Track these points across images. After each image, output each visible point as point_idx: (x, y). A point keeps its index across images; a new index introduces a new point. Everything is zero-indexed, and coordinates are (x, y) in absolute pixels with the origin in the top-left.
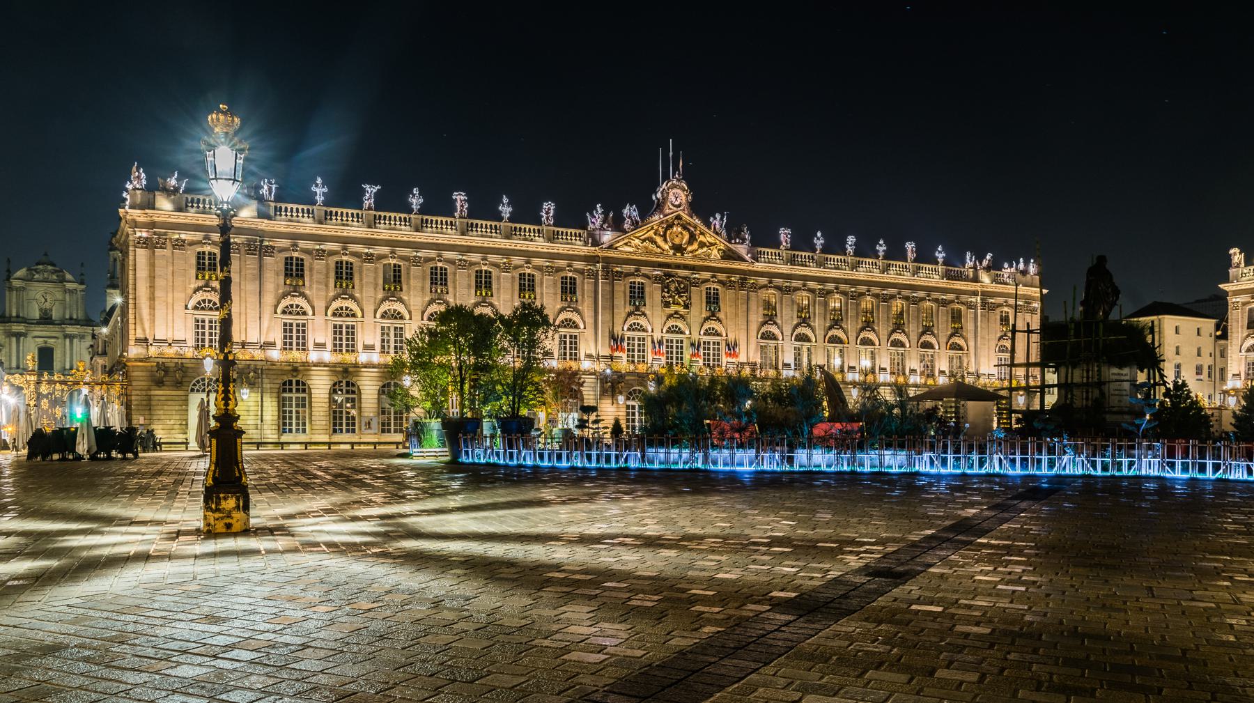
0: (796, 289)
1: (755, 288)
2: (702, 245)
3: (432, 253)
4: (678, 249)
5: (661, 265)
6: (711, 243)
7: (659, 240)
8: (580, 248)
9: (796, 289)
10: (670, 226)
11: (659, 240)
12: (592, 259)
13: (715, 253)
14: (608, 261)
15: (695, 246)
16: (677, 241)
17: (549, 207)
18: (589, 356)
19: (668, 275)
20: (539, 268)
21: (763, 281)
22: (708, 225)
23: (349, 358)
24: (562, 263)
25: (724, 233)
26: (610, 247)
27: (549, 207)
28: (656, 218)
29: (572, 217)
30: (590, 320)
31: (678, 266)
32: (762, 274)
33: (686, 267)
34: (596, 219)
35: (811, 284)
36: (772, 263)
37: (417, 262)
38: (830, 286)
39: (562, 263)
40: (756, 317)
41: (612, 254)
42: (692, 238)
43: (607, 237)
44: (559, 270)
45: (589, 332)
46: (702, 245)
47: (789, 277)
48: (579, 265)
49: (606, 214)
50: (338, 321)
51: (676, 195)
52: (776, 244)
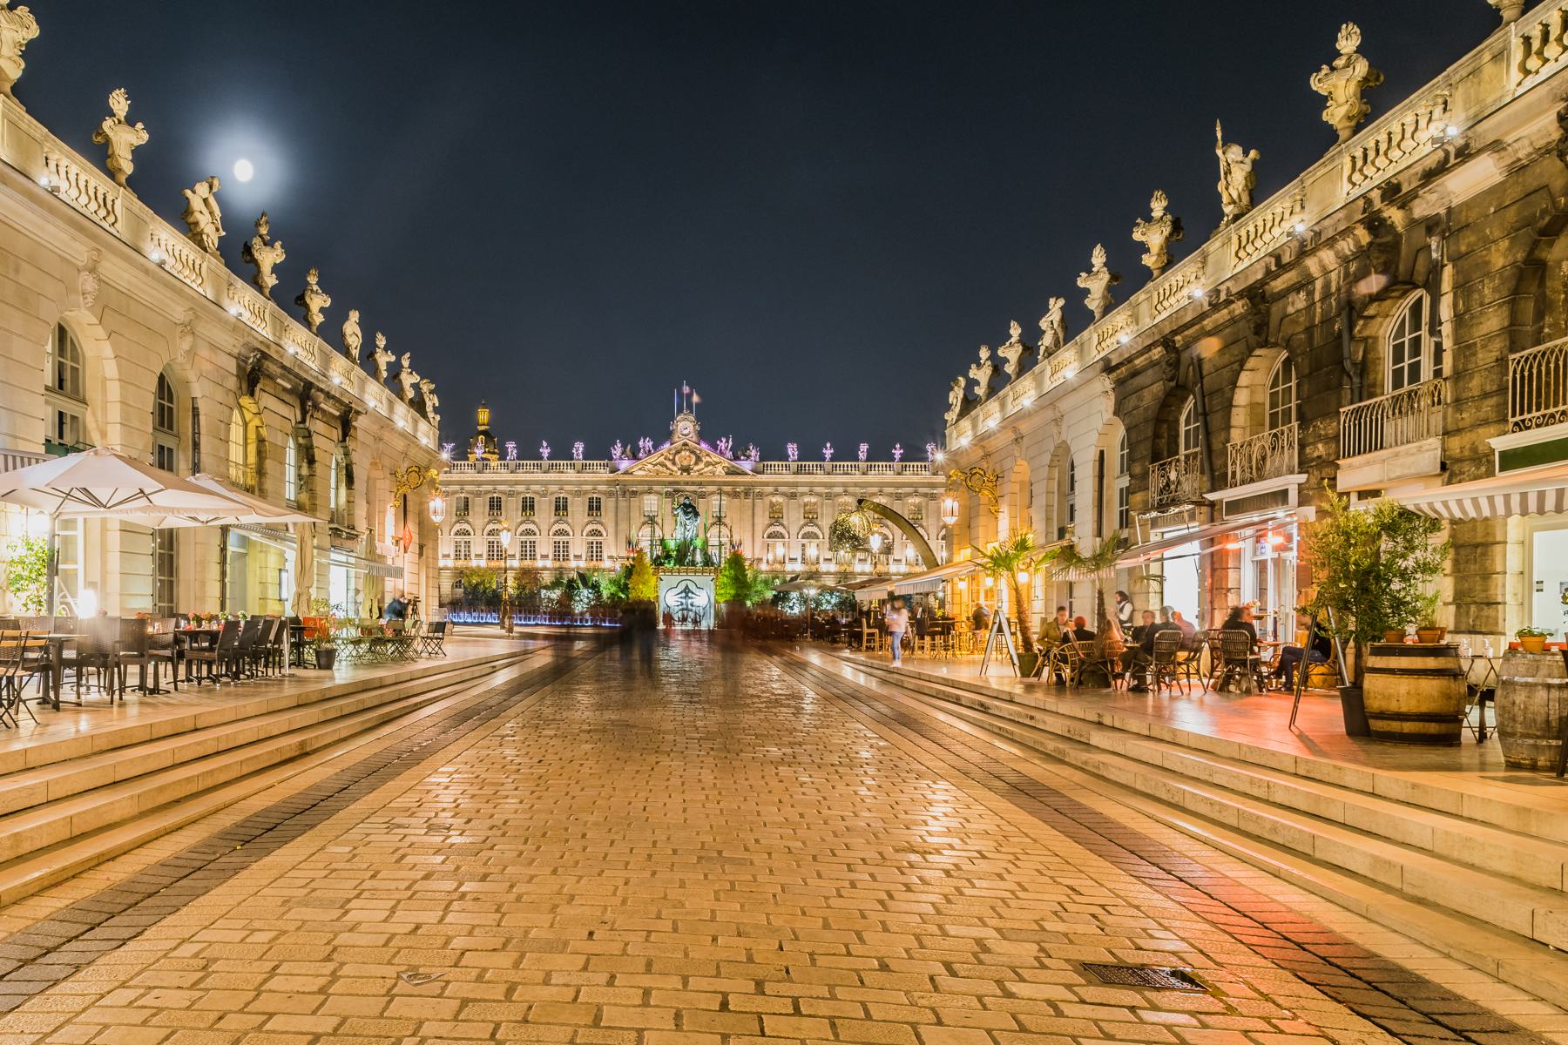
0: (803, 494)
1: (761, 495)
2: (708, 464)
3: (490, 488)
4: (686, 470)
5: (671, 483)
6: (715, 464)
7: (669, 464)
8: (605, 475)
9: (803, 494)
10: (678, 452)
11: (669, 464)
12: (615, 483)
13: (719, 470)
14: (625, 483)
15: (701, 465)
16: (685, 463)
17: (579, 447)
18: (610, 557)
19: (677, 491)
20: (570, 492)
21: (770, 489)
22: (715, 447)
23: (564, 564)
24: (589, 487)
25: (729, 454)
26: (626, 473)
27: (579, 447)
28: (667, 446)
29: (597, 452)
30: (611, 530)
31: (687, 483)
32: (767, 484)
33: (693, 483)
34: (617, 451)
35: (817, 489)
36: (779, 475)
37: (578, 494)
38: (801, 489)
39: (589, 487)
40: (762, 519)
41: (627, 477)
42: (699, 459)
43: (625, 465)
44: (586, 492)
45: (611, 538)
46: (708, 464)
47: (795, 485)
48: (603, 488)
49: (624, 446)
50: (557, 538)
51: (685, 426)
52: (784, 457)
